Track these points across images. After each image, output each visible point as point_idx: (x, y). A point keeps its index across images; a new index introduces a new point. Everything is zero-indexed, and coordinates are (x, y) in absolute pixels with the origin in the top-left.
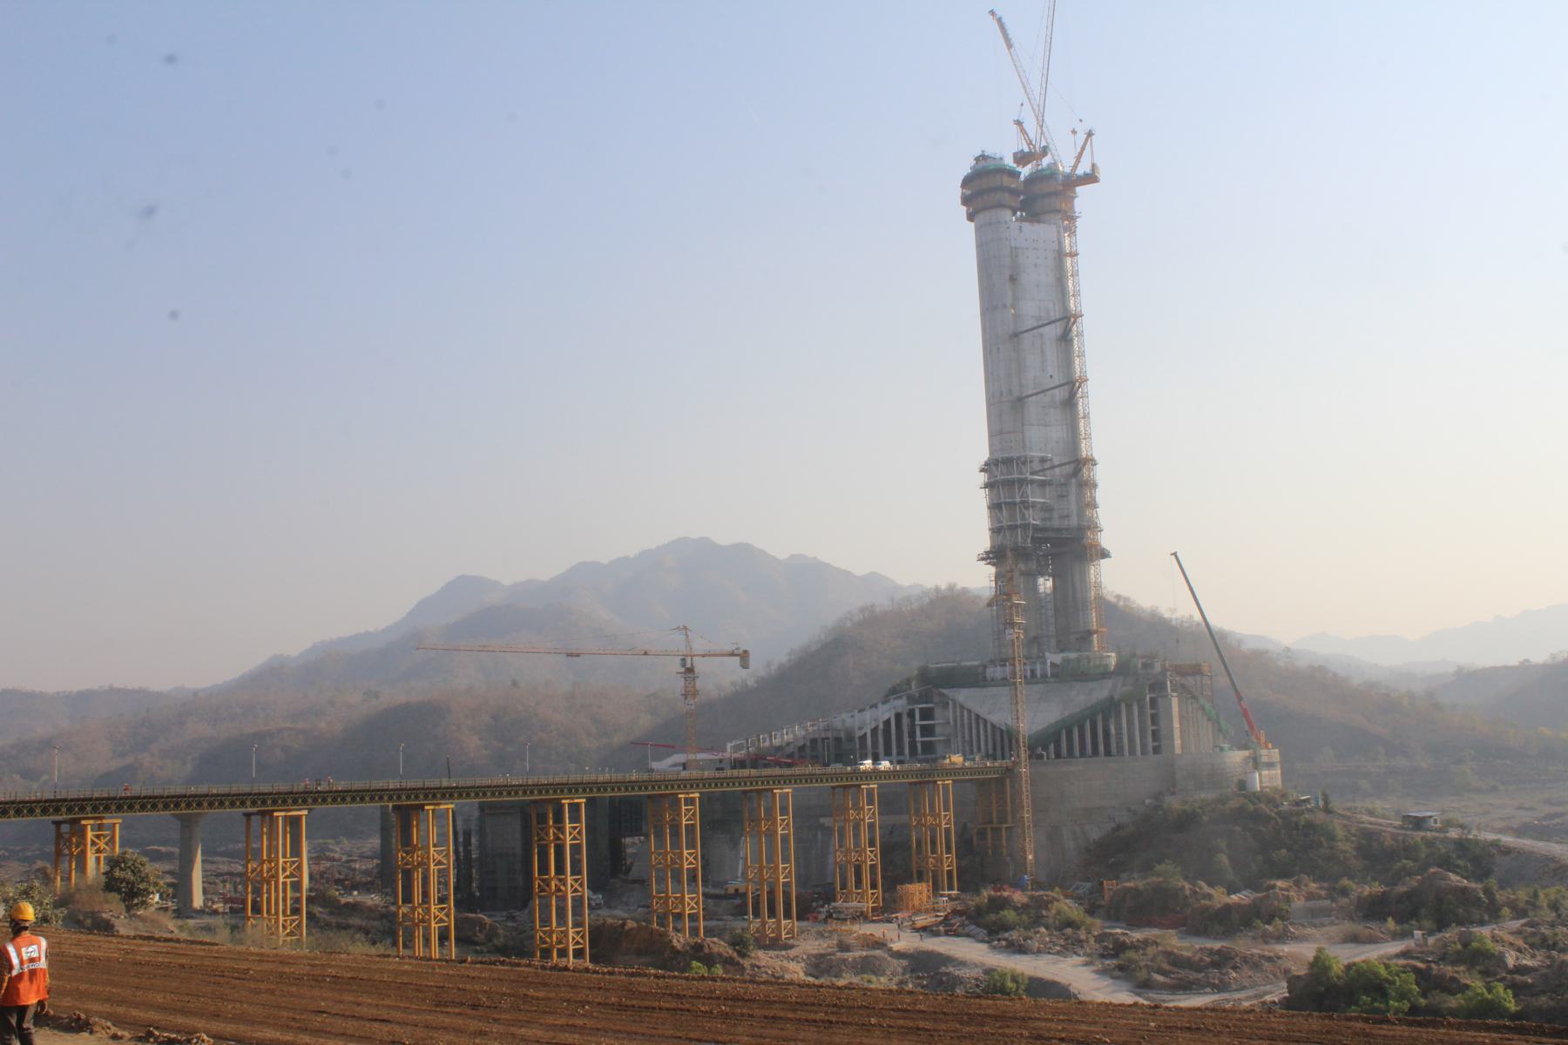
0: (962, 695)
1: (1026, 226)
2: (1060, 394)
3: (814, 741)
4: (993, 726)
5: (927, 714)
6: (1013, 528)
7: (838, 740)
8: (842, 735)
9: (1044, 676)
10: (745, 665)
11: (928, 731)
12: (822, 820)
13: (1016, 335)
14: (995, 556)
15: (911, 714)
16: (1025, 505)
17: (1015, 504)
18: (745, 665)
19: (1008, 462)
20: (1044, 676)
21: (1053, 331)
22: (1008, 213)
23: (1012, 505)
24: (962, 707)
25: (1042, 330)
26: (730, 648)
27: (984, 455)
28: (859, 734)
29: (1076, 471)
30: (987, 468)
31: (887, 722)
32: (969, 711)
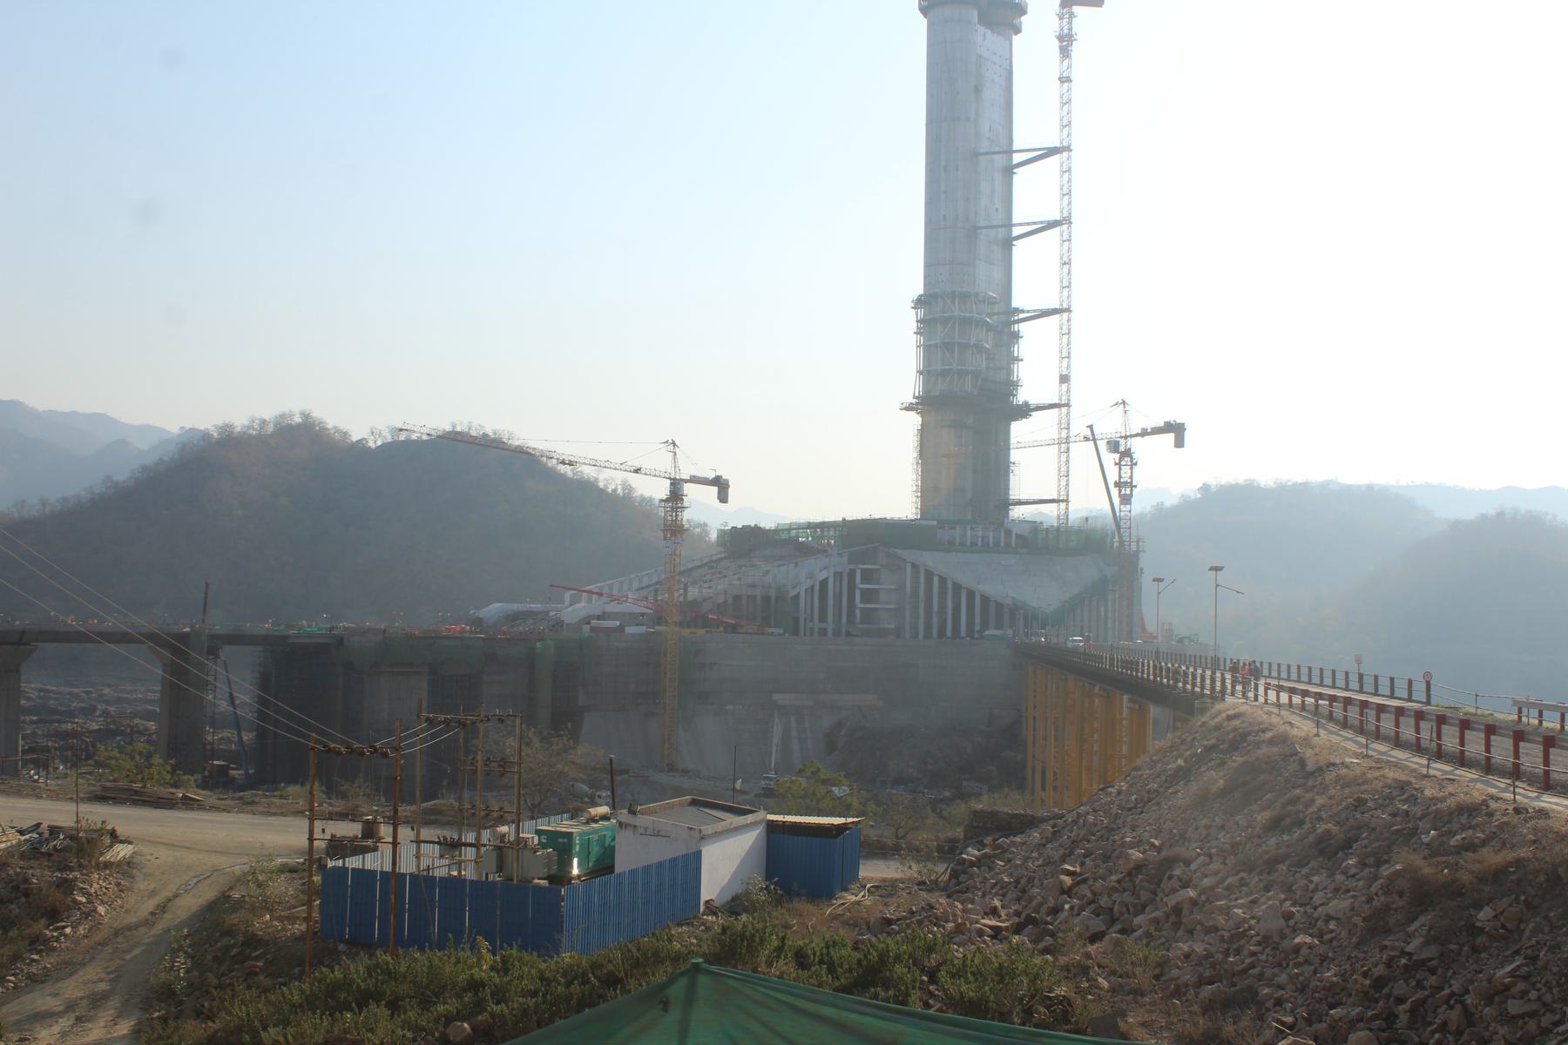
0: (928, 559)
1: (988, 32)
2: (1001, 232)
3: (737, 598)
4: (985, 600)
5: (868, 576)
6: (961, 373)
7: (766, 599)
8: (773, 594)
9: (1008, 544)
10: (723, 498)
11: (868, 596)
12: (776, 697)
13: (976, 155)
14: (925, 404)
15: (852, 574)
16: (979, 348)
17: (967, 345)
18: (723, 498)
19: (964, 297)
20: (1008, 544)
21: (999, 160)
22: (975, 13)
23: (964, 347)
24: (929, 575)
25: (996, 157)
26: (711, 476)
27: (919, 289)
28: (793, 593)
29: (1003, 325)
30: (919, 303)
31: (824, 583)
32: (943, 580)
